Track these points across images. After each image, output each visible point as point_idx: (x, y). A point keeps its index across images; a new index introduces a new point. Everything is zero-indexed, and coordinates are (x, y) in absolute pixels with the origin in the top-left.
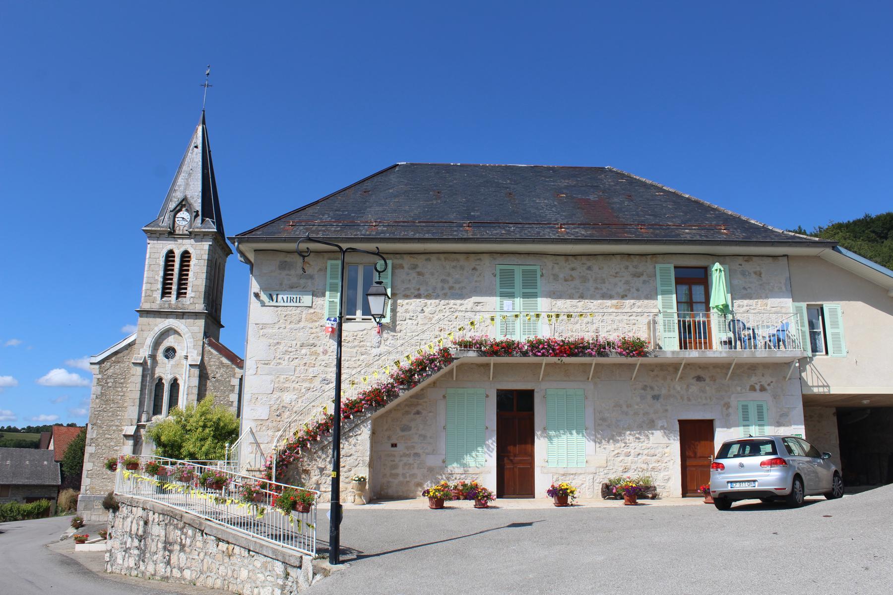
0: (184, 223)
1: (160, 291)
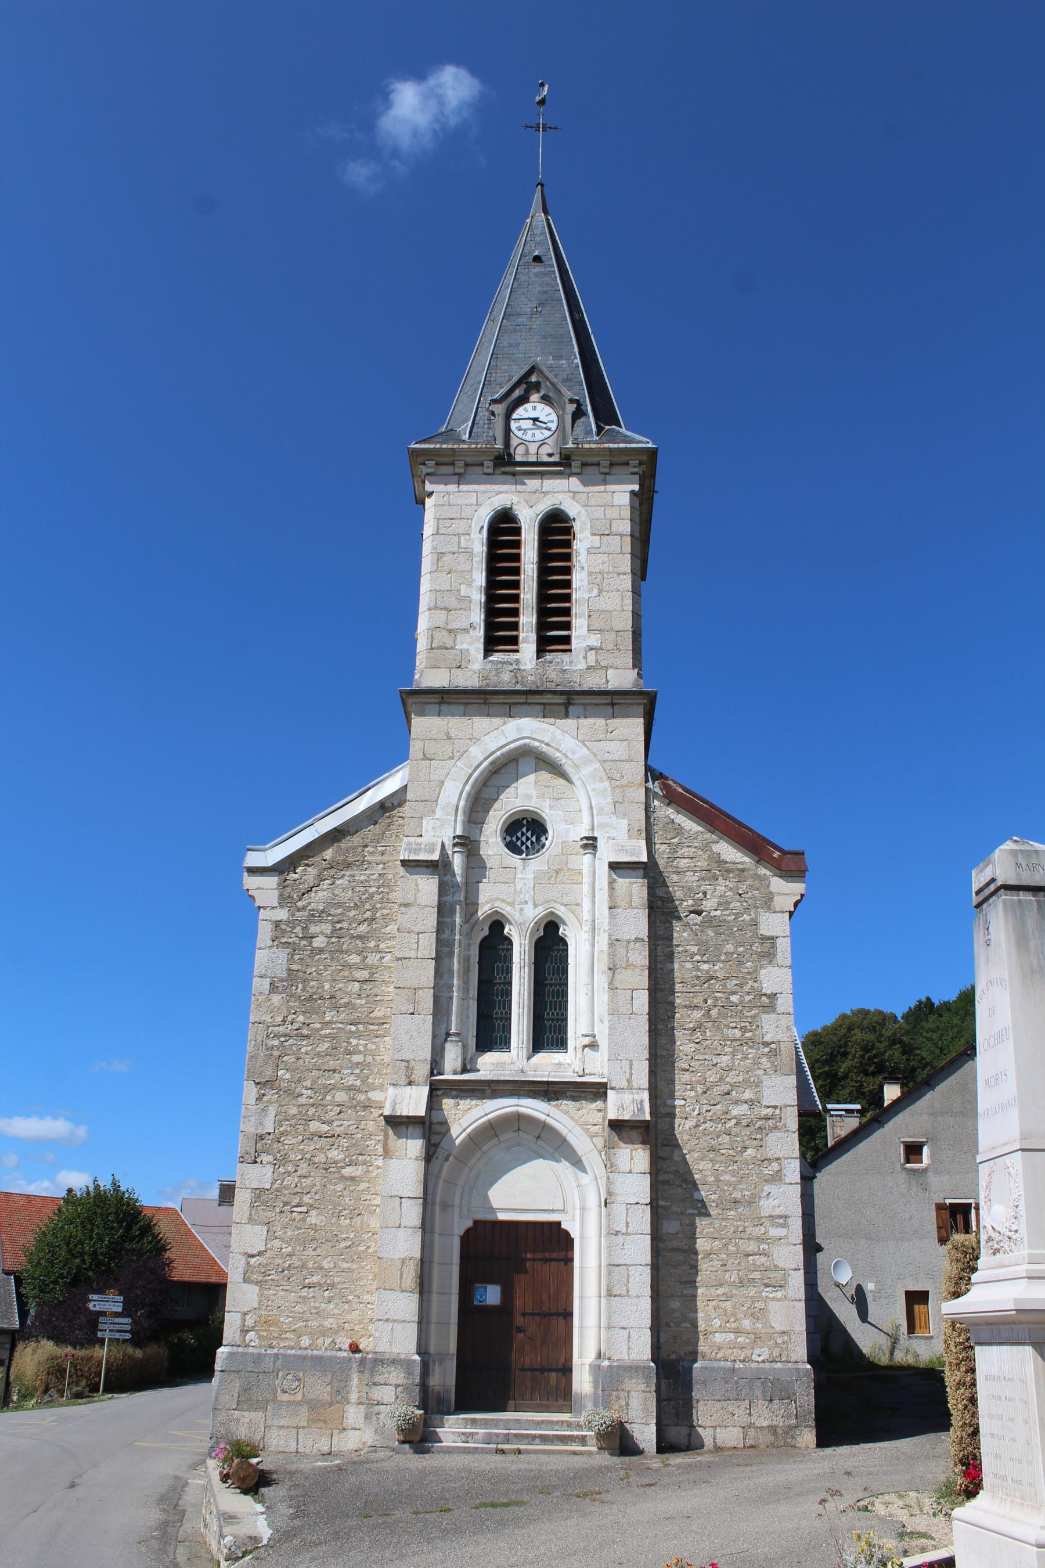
0: (540, 435)
1: (481, 633)
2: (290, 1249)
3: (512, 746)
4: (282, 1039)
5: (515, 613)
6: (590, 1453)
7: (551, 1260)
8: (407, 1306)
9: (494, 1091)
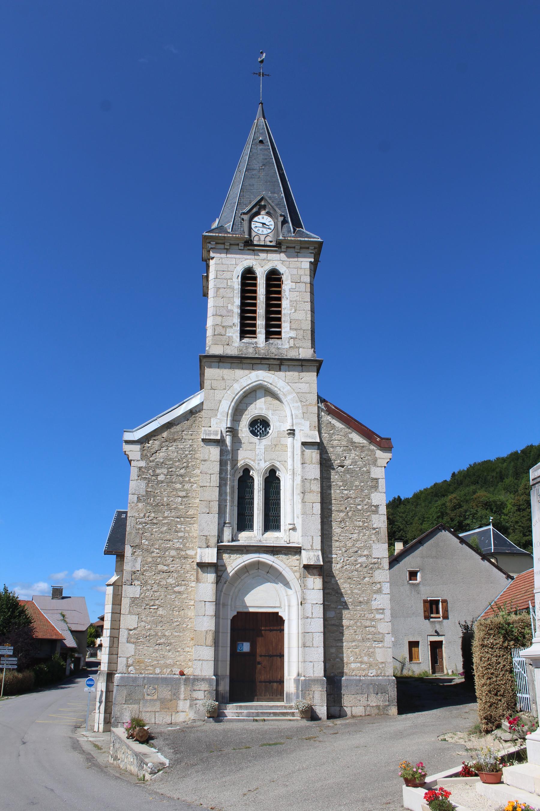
0: (266, 231)
2: (149, 626)
3: (254, 384)
4: (144, 525)
5: (254, 319)
6: (297, 720)
7: (273, 630)
8: (208, 653)
9: (247, 551)
